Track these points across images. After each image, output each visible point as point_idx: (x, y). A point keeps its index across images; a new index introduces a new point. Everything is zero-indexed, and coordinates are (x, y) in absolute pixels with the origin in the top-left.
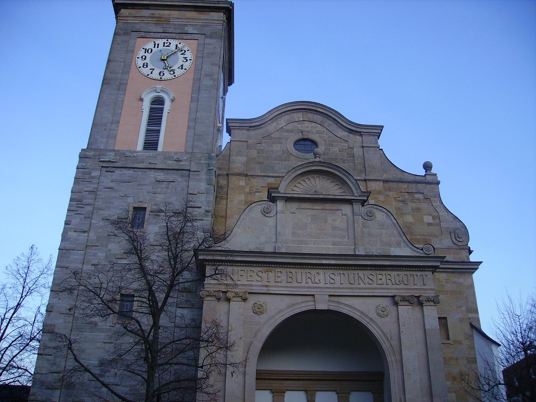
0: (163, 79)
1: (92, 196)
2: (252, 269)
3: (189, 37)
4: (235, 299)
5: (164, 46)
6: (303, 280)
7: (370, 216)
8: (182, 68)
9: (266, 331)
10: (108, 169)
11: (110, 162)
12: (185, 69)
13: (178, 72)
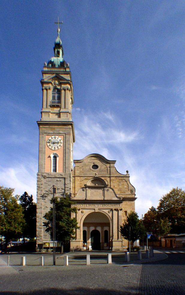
6: (92, 206)
13: (59, 147)
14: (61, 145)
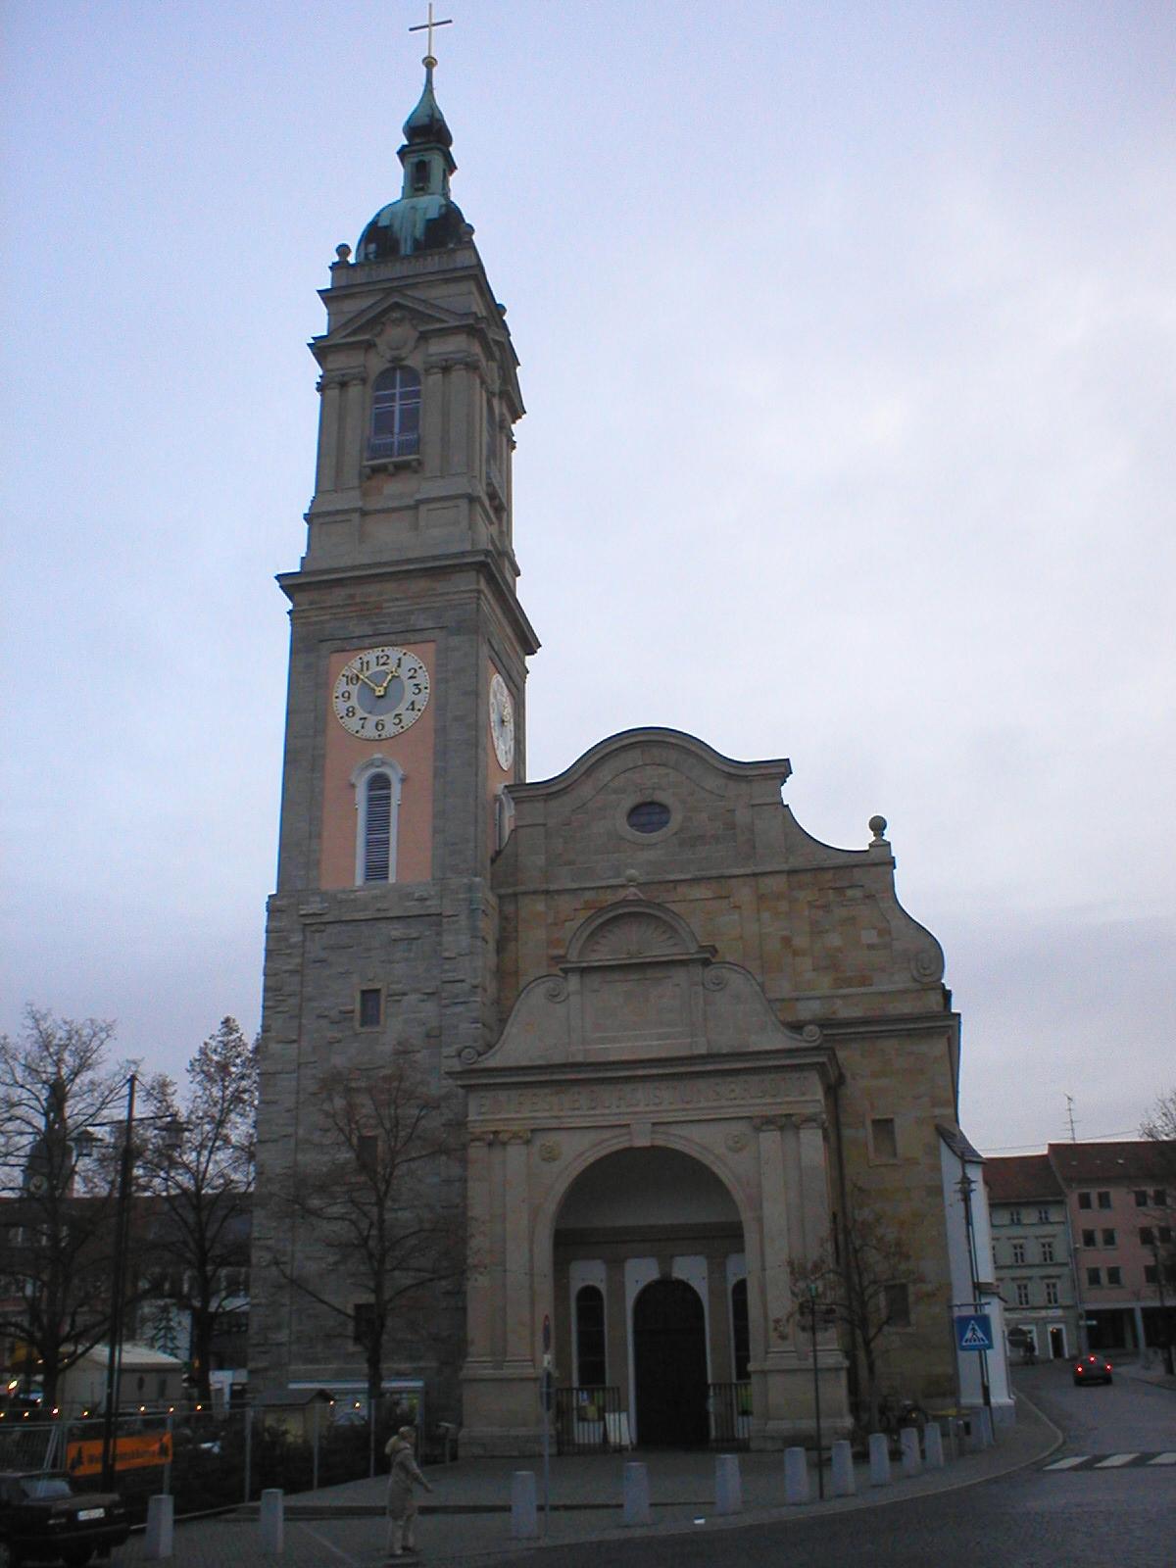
0: (383, 737)
1: (296, 979)
2: (536, 1091)
3: (417, 637)
4: (513, 1141)
5: (378, 665)
7: (720, 984)
8: (413, 709)
9: (561, 1187)
10: (313, 929)
11: (314, 914)
12: (419, 710)
14: (417, 707)
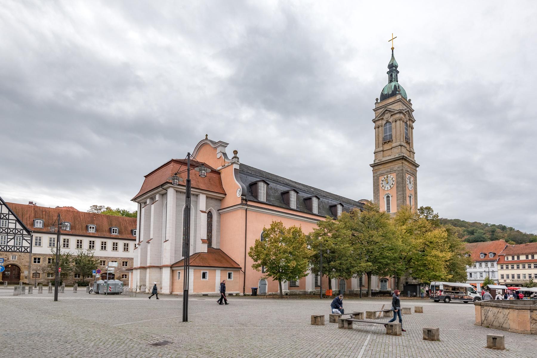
13: (392, 186)
